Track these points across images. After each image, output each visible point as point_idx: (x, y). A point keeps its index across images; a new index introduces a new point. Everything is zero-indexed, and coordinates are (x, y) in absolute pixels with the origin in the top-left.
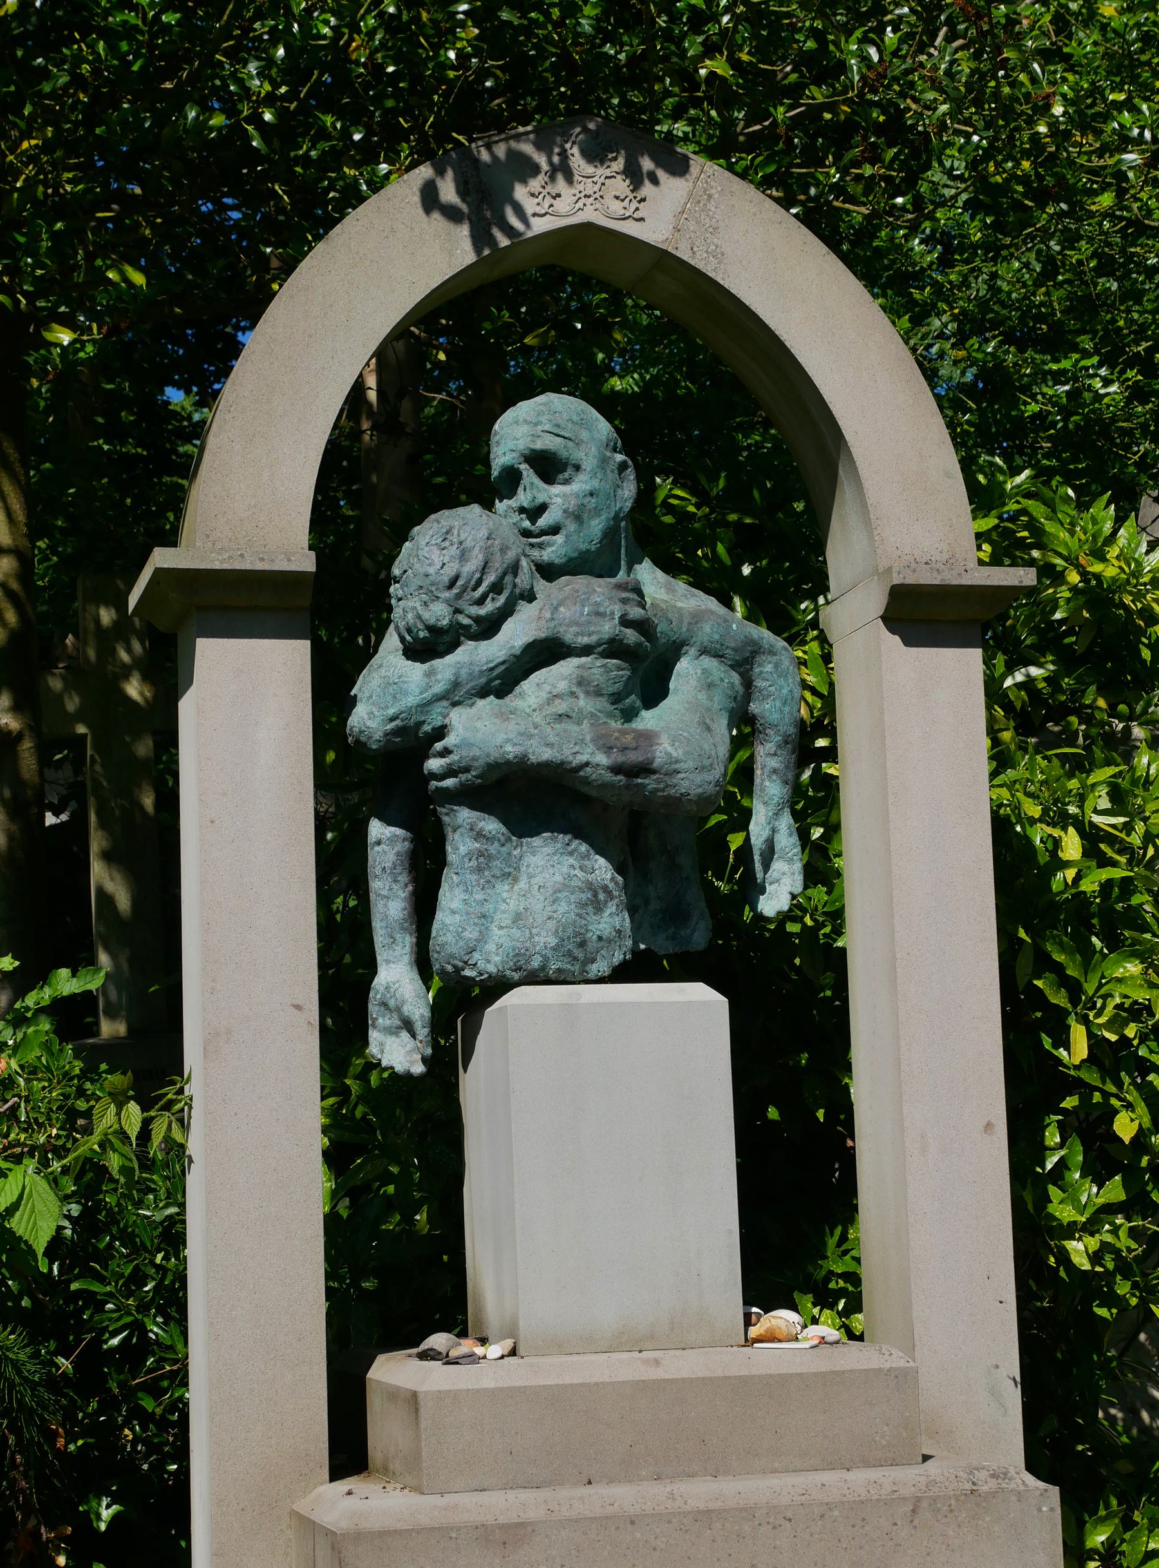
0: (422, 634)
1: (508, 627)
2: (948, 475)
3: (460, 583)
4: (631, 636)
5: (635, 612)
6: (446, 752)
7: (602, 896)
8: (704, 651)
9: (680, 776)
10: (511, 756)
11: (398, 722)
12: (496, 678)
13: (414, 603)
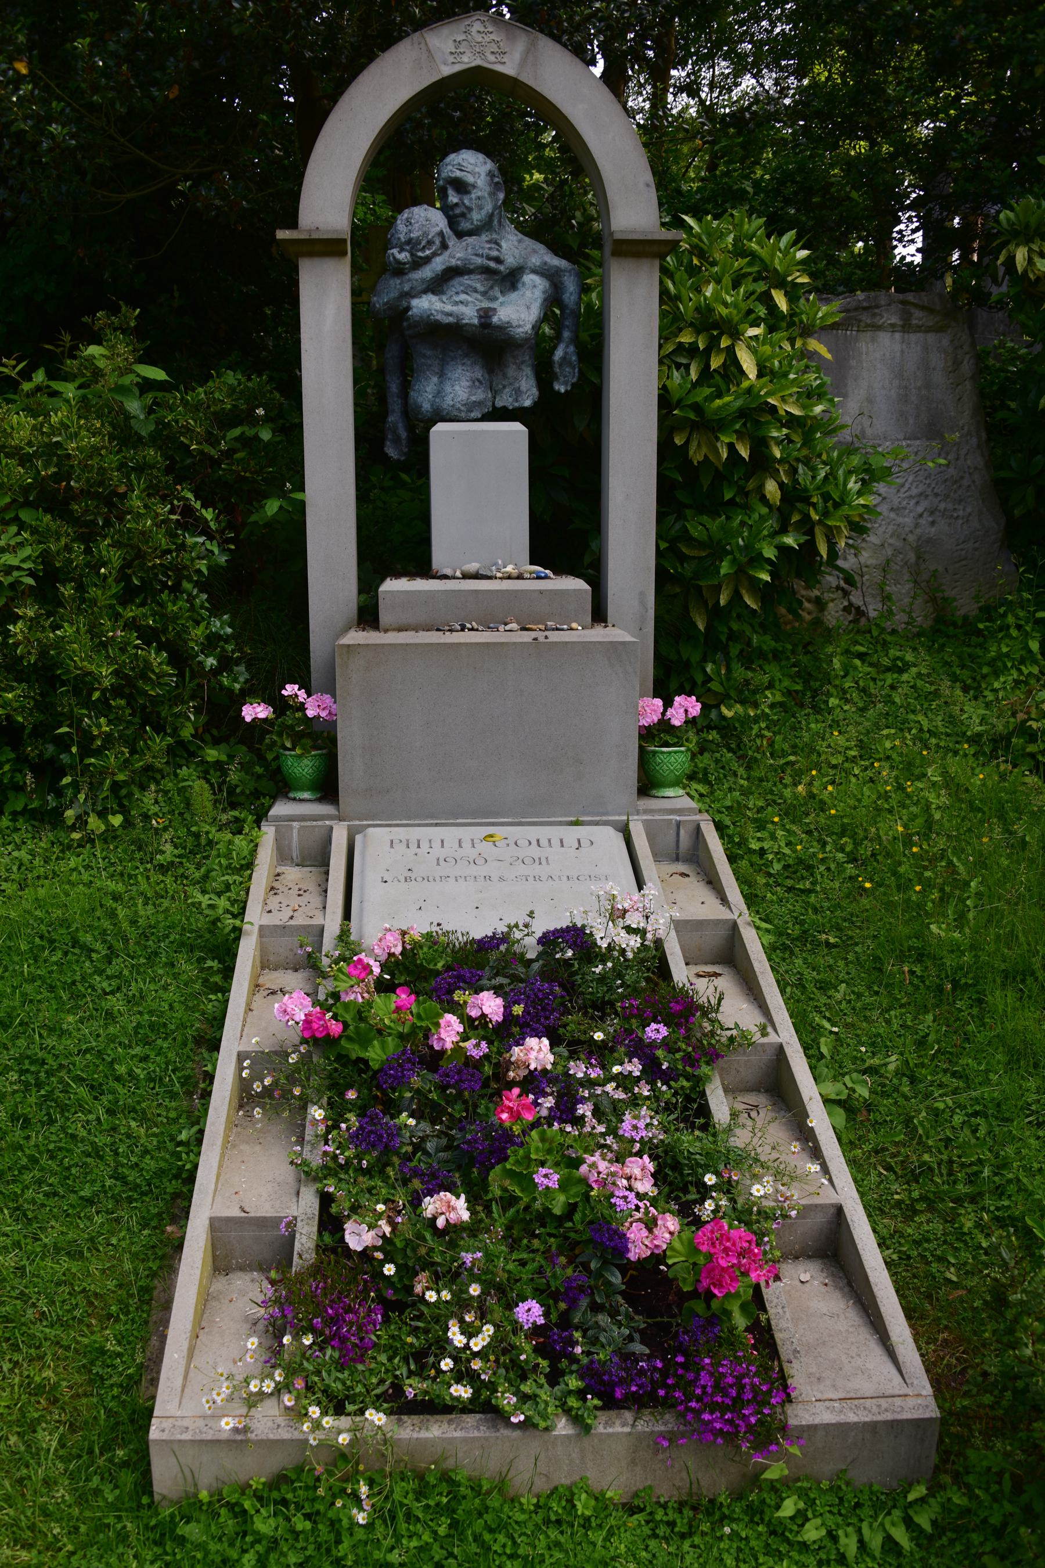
2: (648, 185)
4: (492, 264)
5: (495, 253)
8: (534, 271)
13: (395, 251)
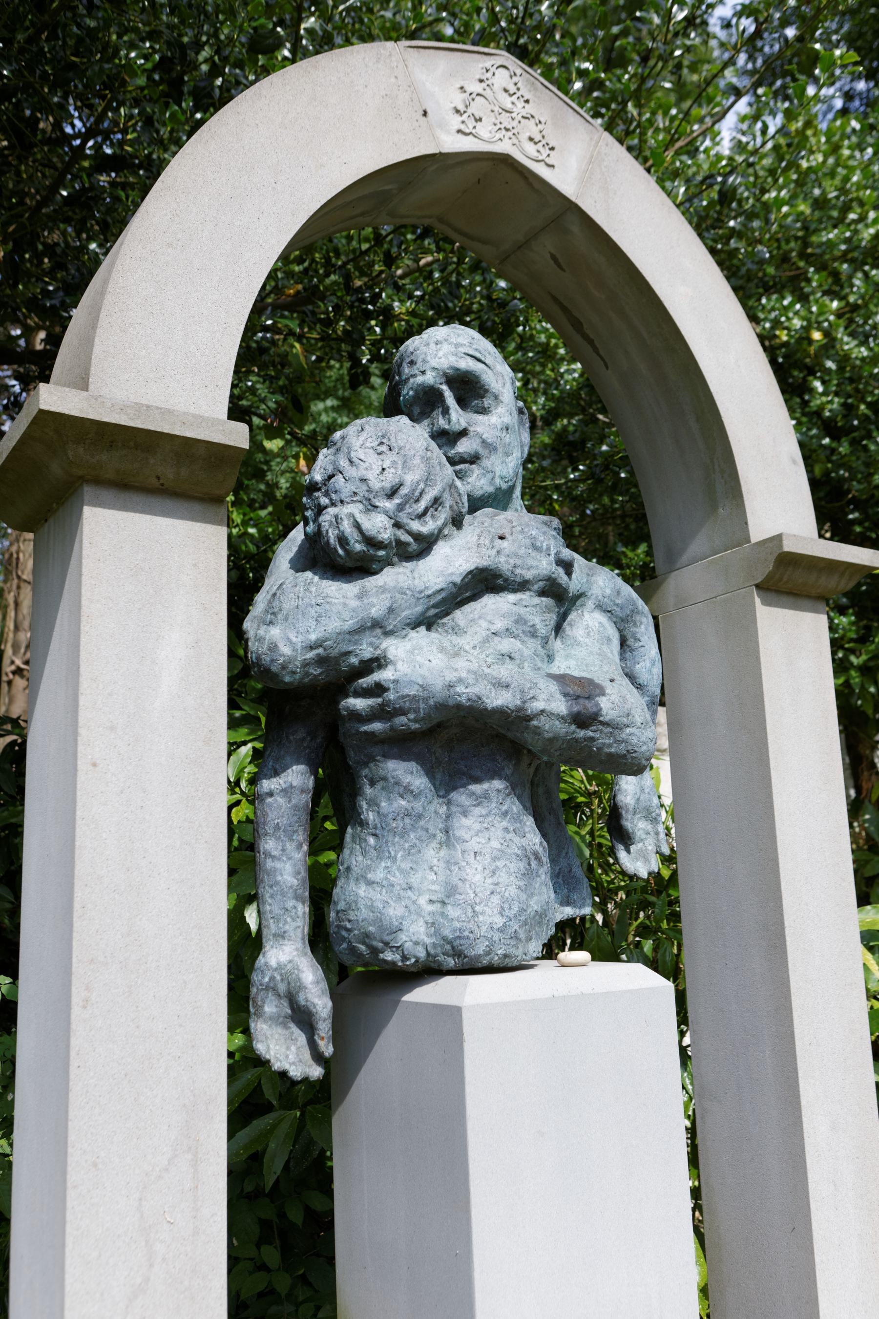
0: (358, 547)
1: (441, 549)
3: (404, 491)
6: (379, 689)
7: (534, 863)
9: (628, 730)
10: (463, 700)
11: (320, 651)
12: (435, 606)
